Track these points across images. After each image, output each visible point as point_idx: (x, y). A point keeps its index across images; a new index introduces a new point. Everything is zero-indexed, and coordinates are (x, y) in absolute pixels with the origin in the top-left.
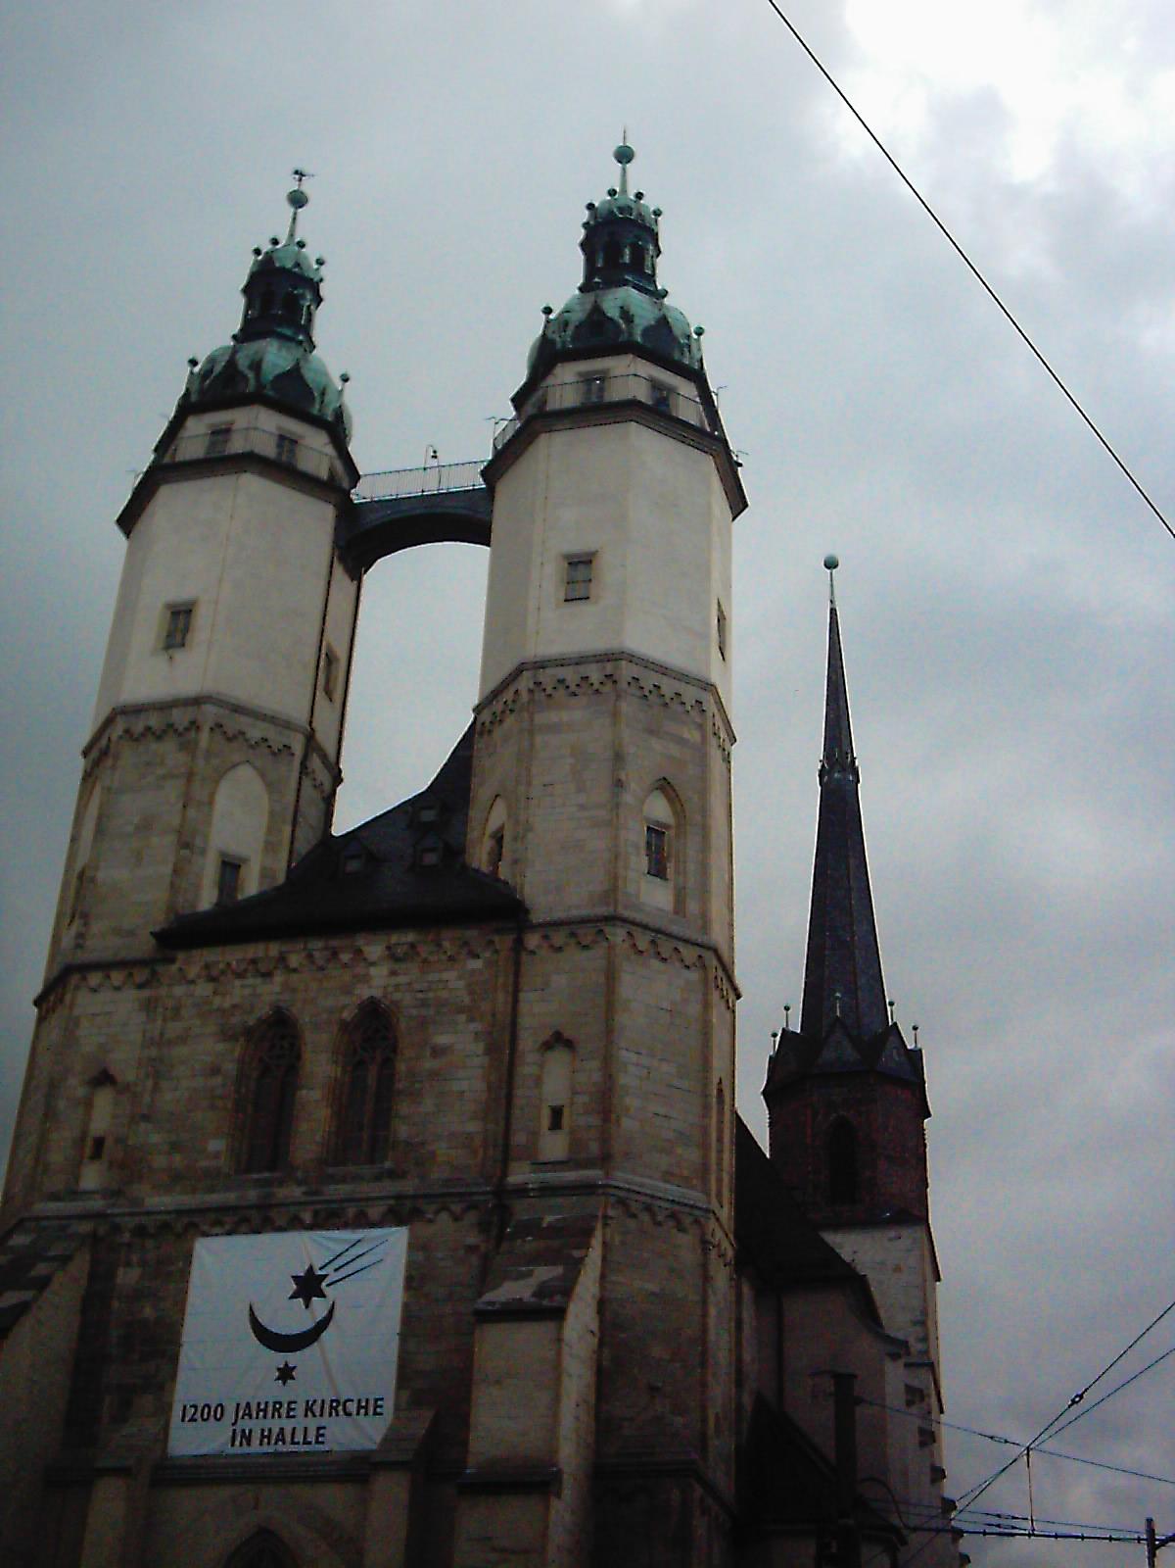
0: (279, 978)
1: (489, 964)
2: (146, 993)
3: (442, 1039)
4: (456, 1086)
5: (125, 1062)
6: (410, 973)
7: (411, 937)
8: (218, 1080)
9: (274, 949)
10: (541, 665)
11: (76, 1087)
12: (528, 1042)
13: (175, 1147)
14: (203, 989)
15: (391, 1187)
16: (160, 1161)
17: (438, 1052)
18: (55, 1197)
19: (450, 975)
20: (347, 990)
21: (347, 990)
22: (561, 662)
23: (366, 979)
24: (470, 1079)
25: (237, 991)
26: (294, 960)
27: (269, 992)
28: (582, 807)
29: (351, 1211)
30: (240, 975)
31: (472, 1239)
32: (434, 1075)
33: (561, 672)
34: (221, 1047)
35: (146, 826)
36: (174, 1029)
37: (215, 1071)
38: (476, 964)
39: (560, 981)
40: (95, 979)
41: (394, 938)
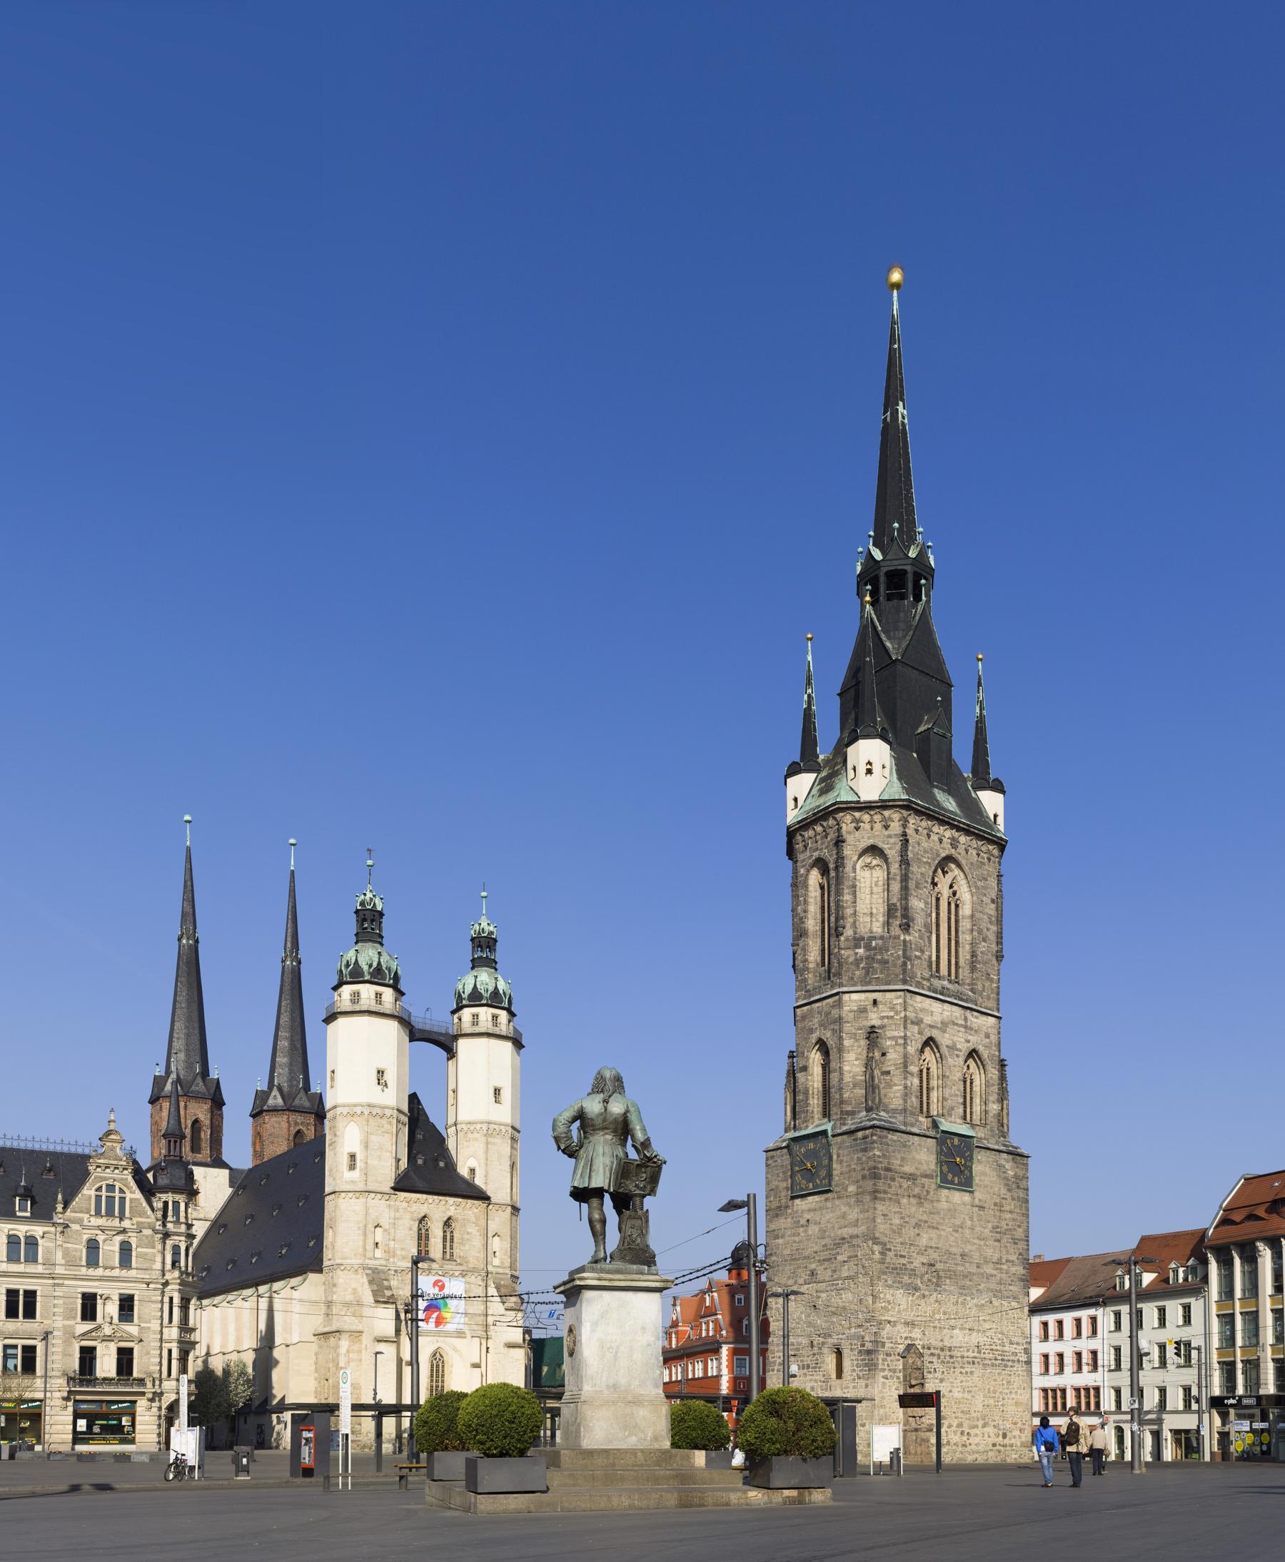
0: (426, 1205)
1: (480, 1211)
2: (388, 1202)
3: (469, 1230)
4: (475, 1243)
5: (385, 1222)
6: (460, 1210)
7: (460, 1200)
8: (412, 1232)
9: (425, 1196)
10: (489, 1123)
11: (371, 1227)
12: (490, 1235)
13: (403, 1249)
14: (405, 1204)
15: (462, 1268)
16: (399, 1253)
17: (468, 1233)
18: (370, 1259)
19: (470, 1212)
20: (445, 1212)
21: (445, 1212)
22: (495, 1124)
23: (449, 1210)
24: (477, 1242)
25: (415, 1207)
26: (430, 1201)
27: (423, 1210)
28: (501, 1170)
29: (451, 1272)
30: (416, 1202)
31: (481, 1283)
32: (468, 1240)
33: (496, 1127)
34: (412, 1223)
35: (381, 1148)
36: (397, 1215)
37: (411, 1229)
38: (477, 1210)
39: (497, 1219)
40: (373, 1195)
41: (456, 1199)
